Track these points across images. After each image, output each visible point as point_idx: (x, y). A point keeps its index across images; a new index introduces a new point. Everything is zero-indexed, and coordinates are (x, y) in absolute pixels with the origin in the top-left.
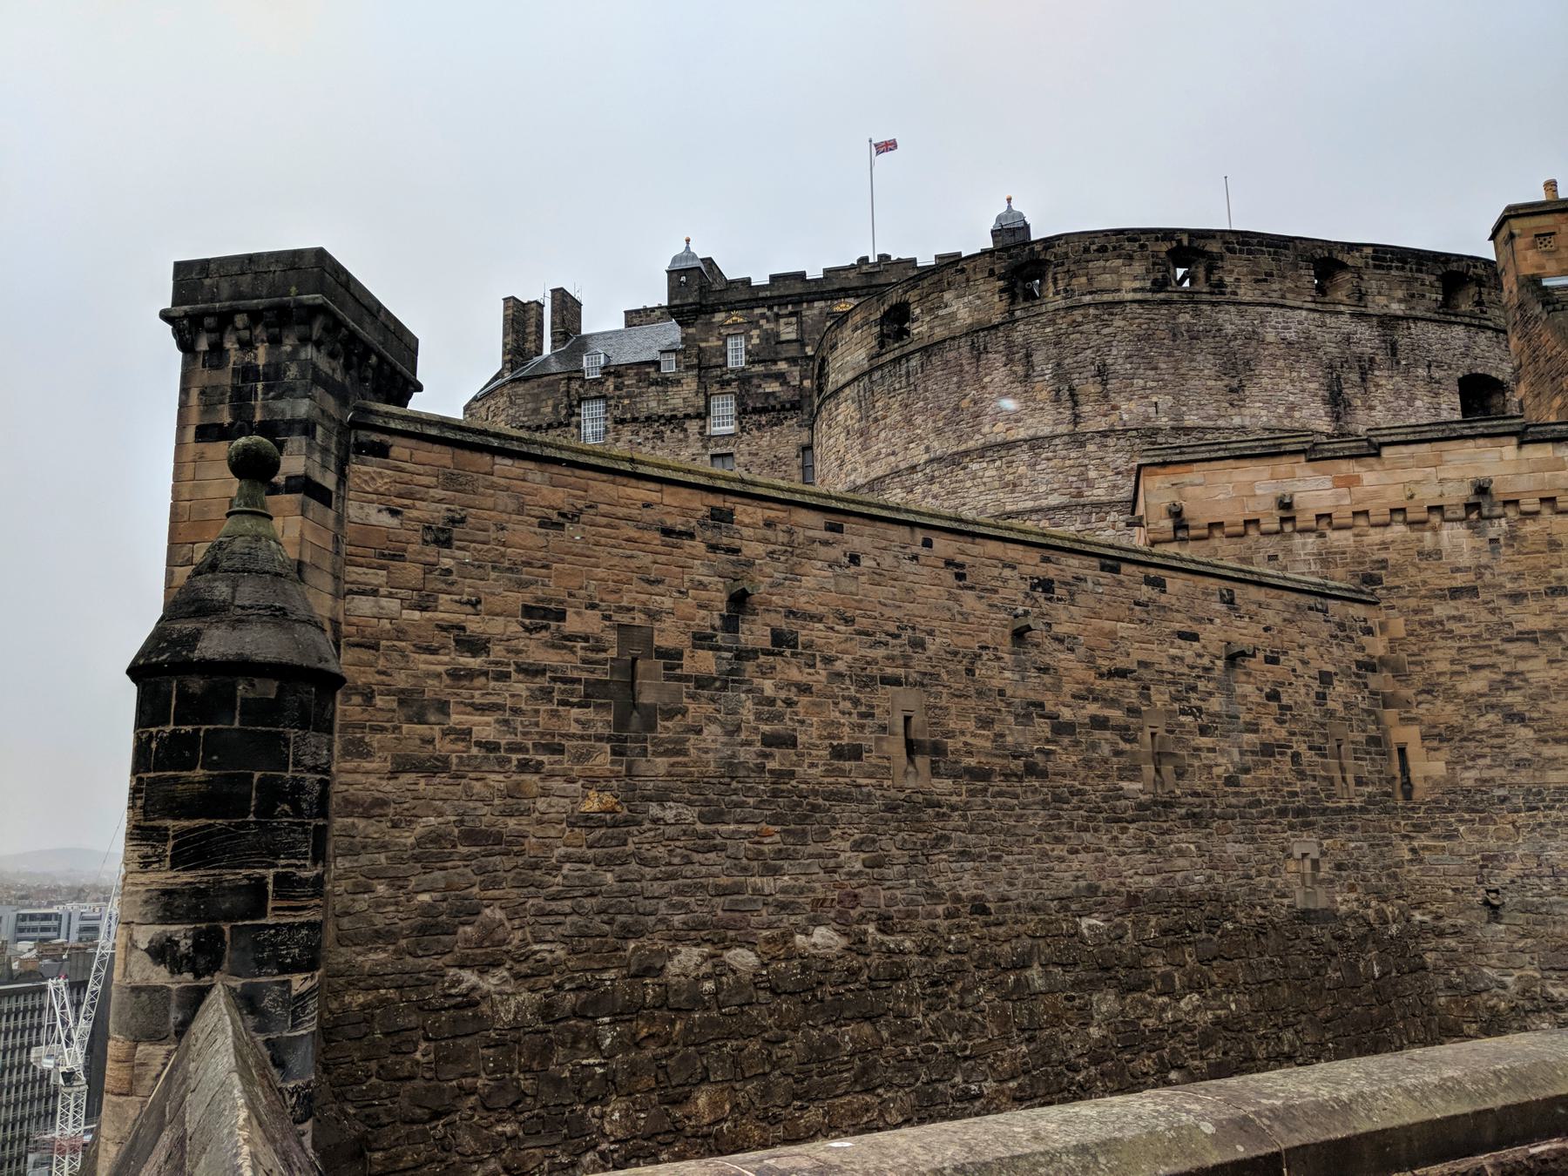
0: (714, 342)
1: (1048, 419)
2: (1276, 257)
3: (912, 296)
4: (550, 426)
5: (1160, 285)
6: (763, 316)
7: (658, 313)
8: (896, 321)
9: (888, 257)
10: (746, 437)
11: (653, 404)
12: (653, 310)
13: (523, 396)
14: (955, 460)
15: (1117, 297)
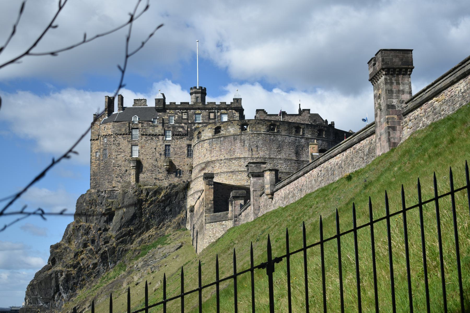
0: (166, 117)
1: (247, 154)
2: (288, 126)
3: (222, 125)
4: (124, 134)
5: (268, 131)
6: (178, 112)
7: (143, 101)
8: (217, 130)
9: (202, 87)
10: (174, 141)
11: (151, 131)
12: (142, 100)
13: (116, 126)
14: (230, 160)
15: (260, 132)
